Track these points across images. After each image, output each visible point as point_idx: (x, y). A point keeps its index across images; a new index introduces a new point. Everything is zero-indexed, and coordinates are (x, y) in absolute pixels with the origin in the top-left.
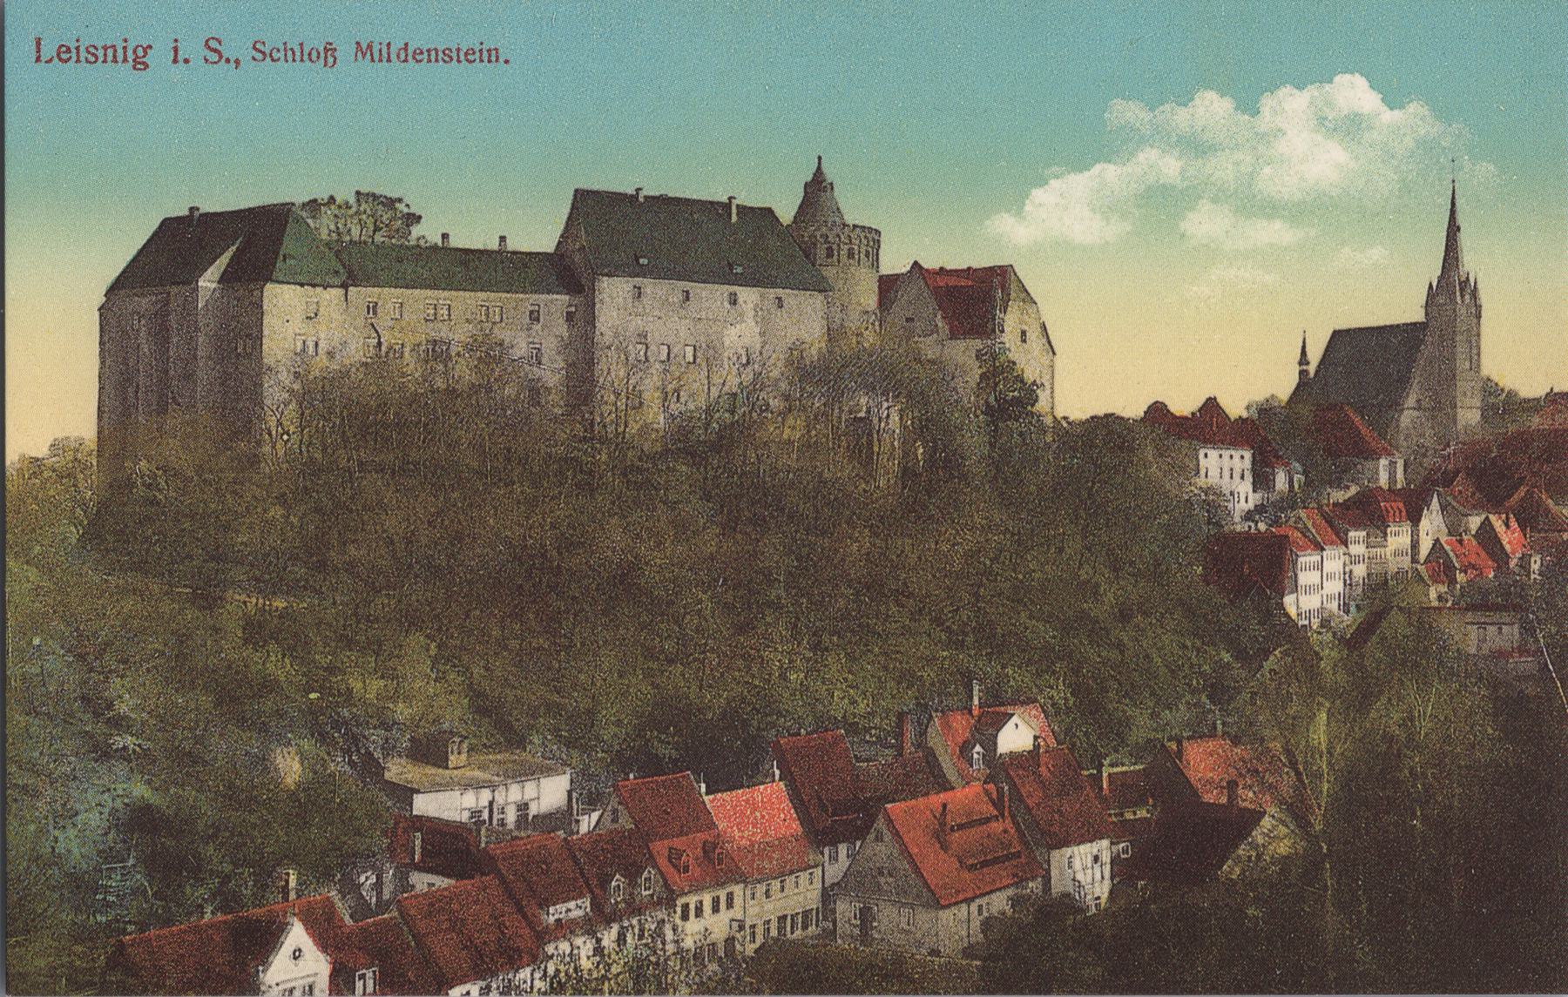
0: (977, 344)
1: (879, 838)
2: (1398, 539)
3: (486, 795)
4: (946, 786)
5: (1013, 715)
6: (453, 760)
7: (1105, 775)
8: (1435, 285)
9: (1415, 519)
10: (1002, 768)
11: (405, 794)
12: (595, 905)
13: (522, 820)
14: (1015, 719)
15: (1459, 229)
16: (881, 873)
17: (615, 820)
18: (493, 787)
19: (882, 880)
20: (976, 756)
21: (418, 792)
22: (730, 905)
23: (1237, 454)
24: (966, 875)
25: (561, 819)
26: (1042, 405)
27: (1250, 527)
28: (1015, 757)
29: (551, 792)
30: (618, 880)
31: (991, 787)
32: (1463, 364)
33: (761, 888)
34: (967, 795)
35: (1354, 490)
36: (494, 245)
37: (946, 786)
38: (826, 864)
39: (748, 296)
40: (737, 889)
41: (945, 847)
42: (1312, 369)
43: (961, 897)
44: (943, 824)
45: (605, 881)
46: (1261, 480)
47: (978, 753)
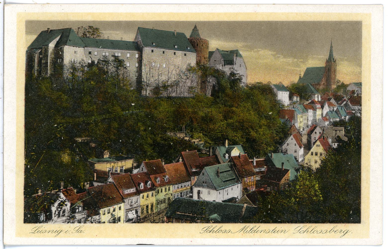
0: (230, 66)
1: (203, 174)
2: (319, 112)
3: (112, 164)
4: (219, 163)
5: (234, 147)
6: (105, 157)
7: (255, 161)
8: (327, 59)
9: (322, 107)
10: (231, 159)
11: (93, 165)
12: (137, 189)
13: (121, 171)
14: (235, 148)
15: (332, 47)
16: (203, 182)
17: (142, 170)
18: (114, 163)
19: (204, 184)
20: (226, 157)
21: (96, 164)
22: (169, 190)
23: (286, 93)
24: (223, 183)
25: (129, 171)
26: (244, 80)
27: (288, 108)
28: (235, 157)
29: (128, 164)
30: (142, 184)
31: (229, 163)
32: (333, 76)
33: (176, 186)
34: (224, 165)
35: (310, 101)
36: (120, 39)
37: (219, 163)
38: (192, 181)
39: (179, 53)
40: (171, 186)
41: (218, 176)
42: (302, 76)
43: (222, 188)
44: (218, 172)
45: (139, 184)
46: (291, 98)
47: (227, 156)
